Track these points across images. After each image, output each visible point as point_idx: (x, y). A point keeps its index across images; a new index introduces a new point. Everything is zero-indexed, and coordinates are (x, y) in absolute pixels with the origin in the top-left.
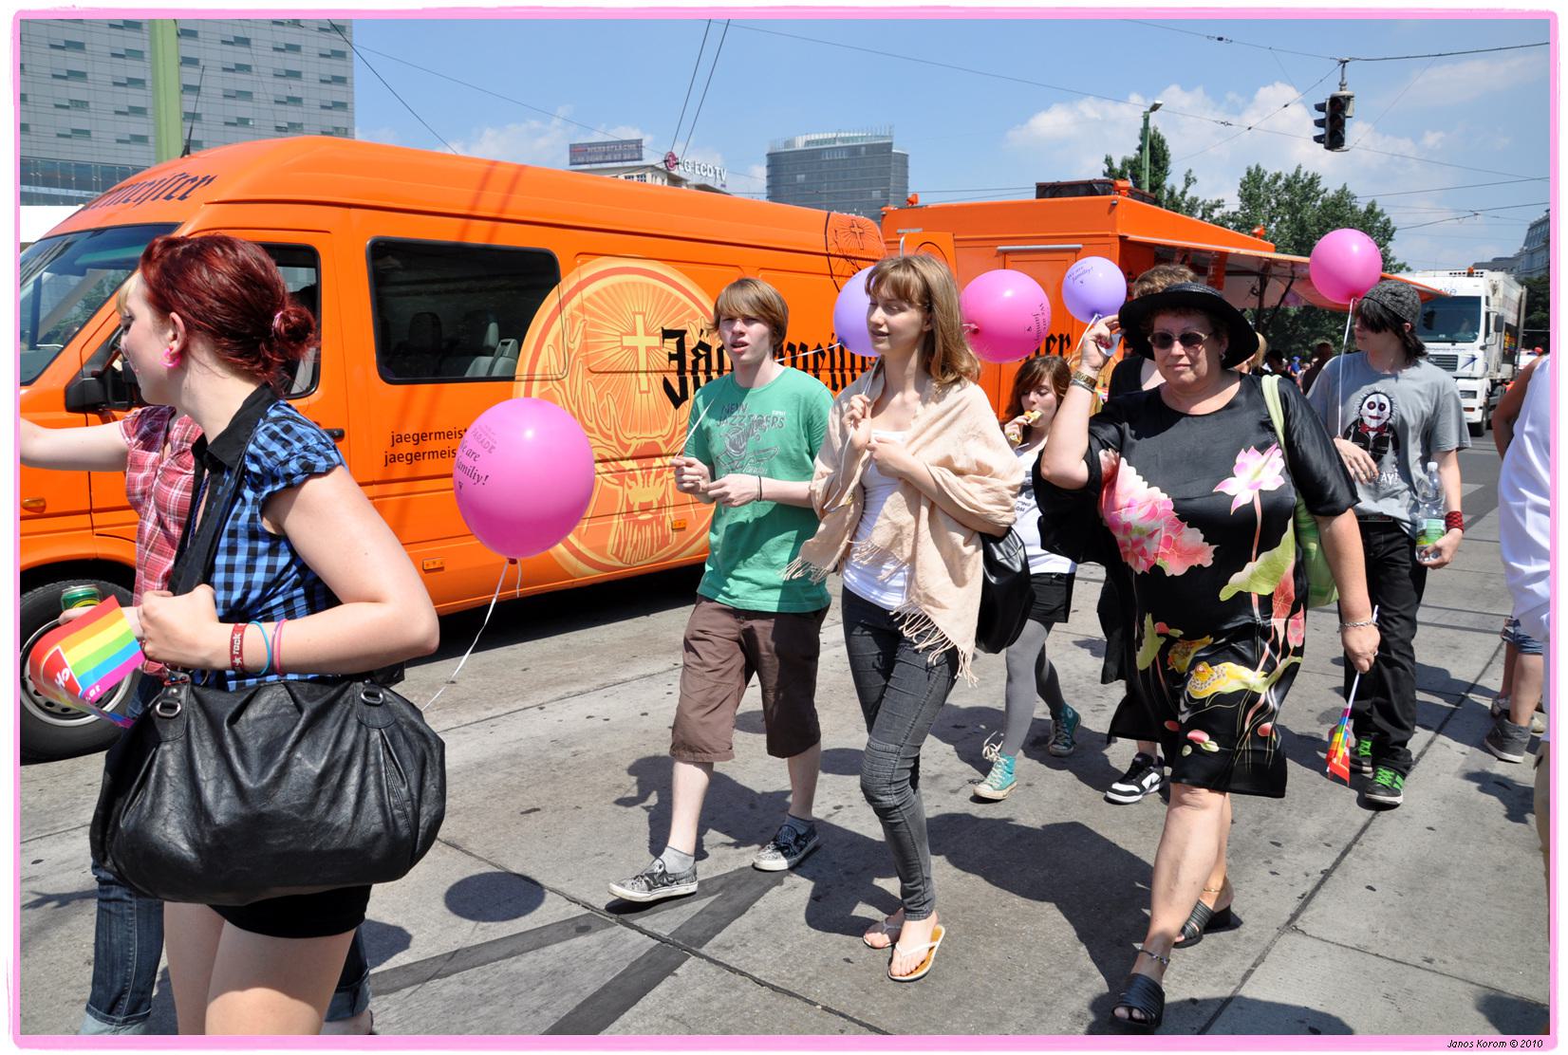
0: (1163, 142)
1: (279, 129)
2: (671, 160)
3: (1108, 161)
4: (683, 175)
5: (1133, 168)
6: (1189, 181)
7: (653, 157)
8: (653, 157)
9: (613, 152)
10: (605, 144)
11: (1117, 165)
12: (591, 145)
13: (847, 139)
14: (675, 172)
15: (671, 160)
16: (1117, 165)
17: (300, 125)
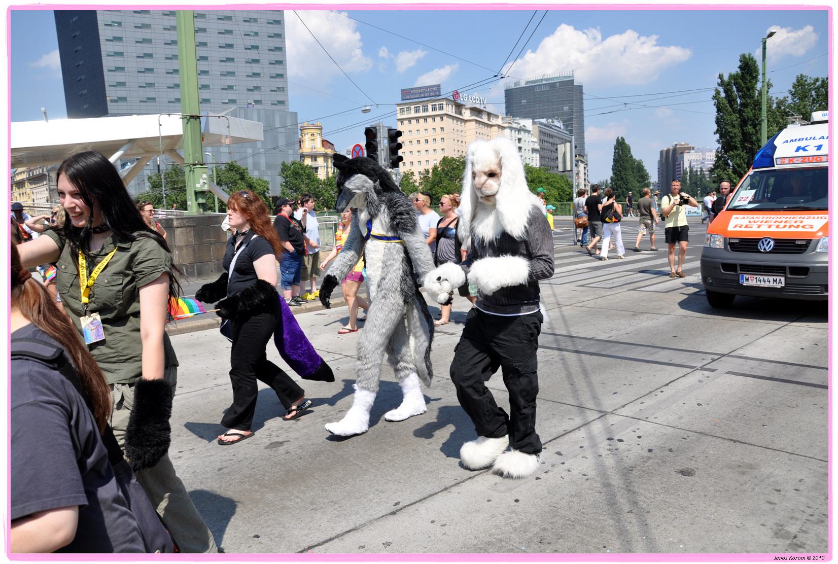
0: (755, 62)
1: (249, 90)
2: (456, 94)
3: (721, 77)
4: (462, 103)
5: (735, 79)
6: (769, 86)
7: (446, 92)
8: (446, 92)
9: (425, 92)
10: (420, 88)
11: (726, 78)
12: (412, 89)
13: (552, 79)
14: (459, 101)
15: (456, 94)
16: (726, 78)
17: (259, 88)
